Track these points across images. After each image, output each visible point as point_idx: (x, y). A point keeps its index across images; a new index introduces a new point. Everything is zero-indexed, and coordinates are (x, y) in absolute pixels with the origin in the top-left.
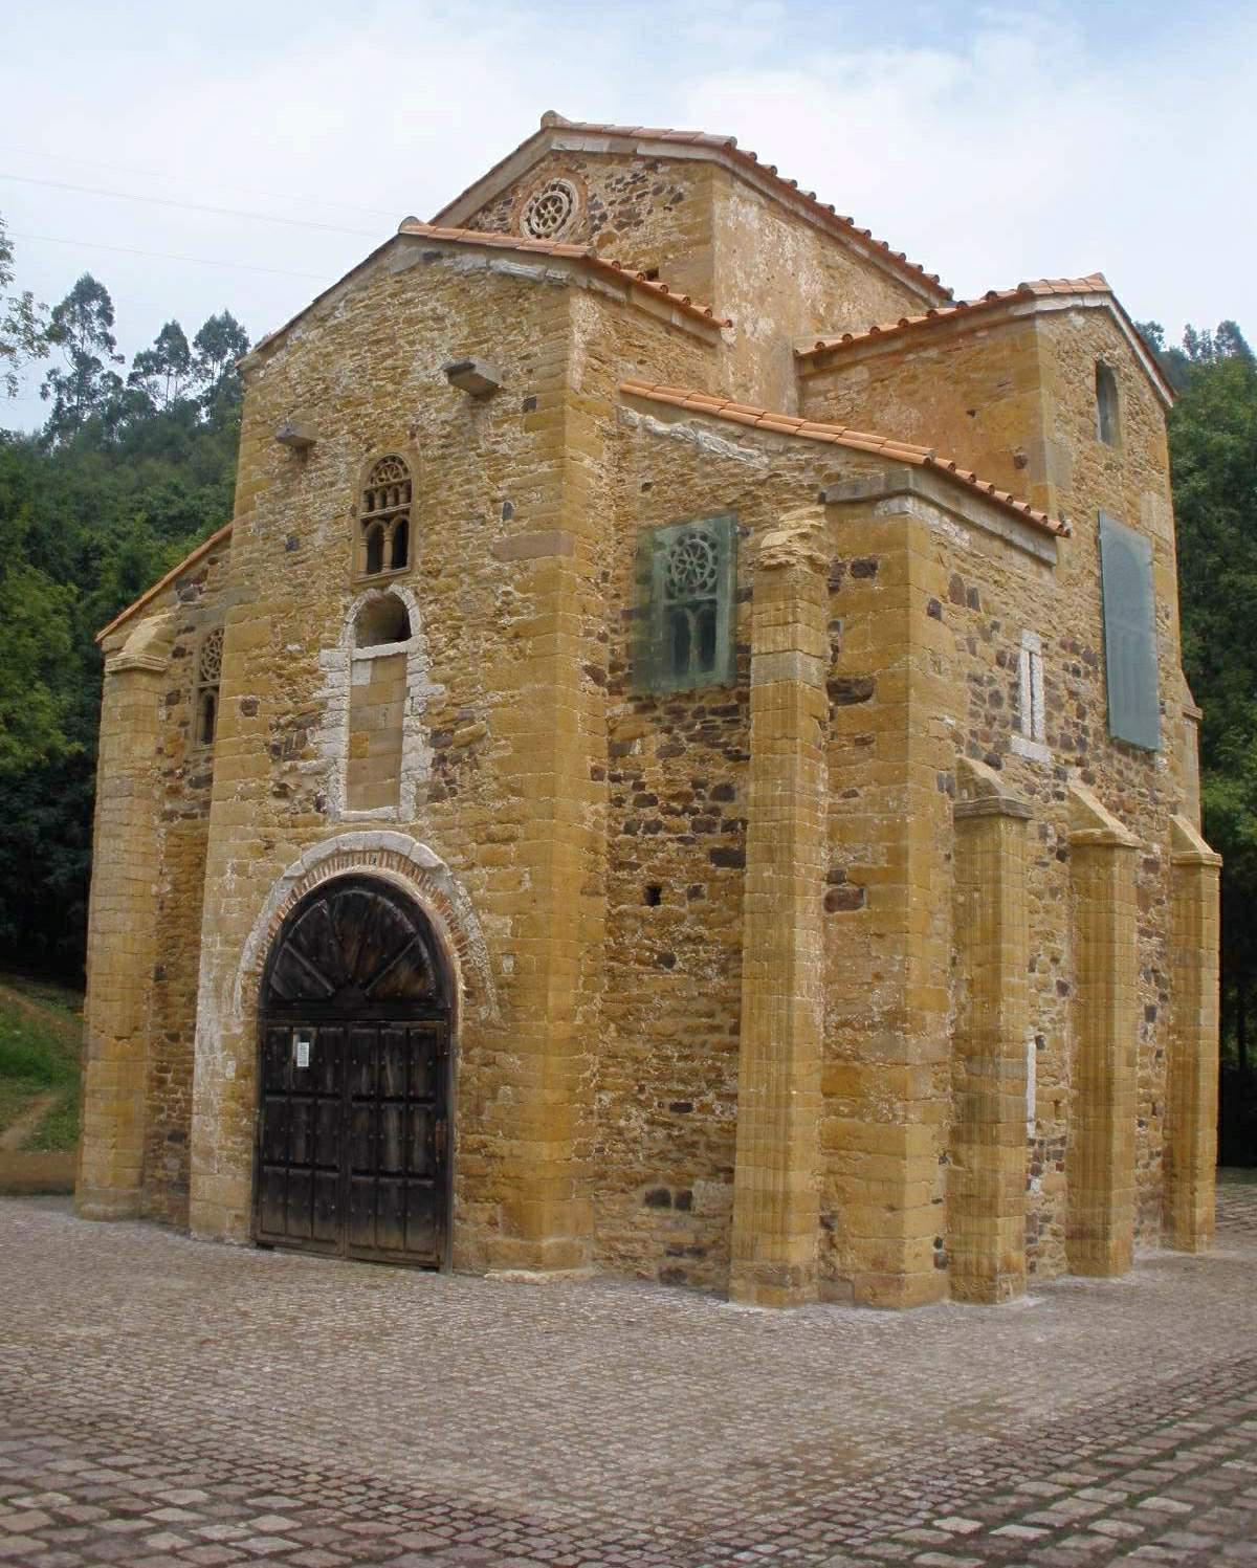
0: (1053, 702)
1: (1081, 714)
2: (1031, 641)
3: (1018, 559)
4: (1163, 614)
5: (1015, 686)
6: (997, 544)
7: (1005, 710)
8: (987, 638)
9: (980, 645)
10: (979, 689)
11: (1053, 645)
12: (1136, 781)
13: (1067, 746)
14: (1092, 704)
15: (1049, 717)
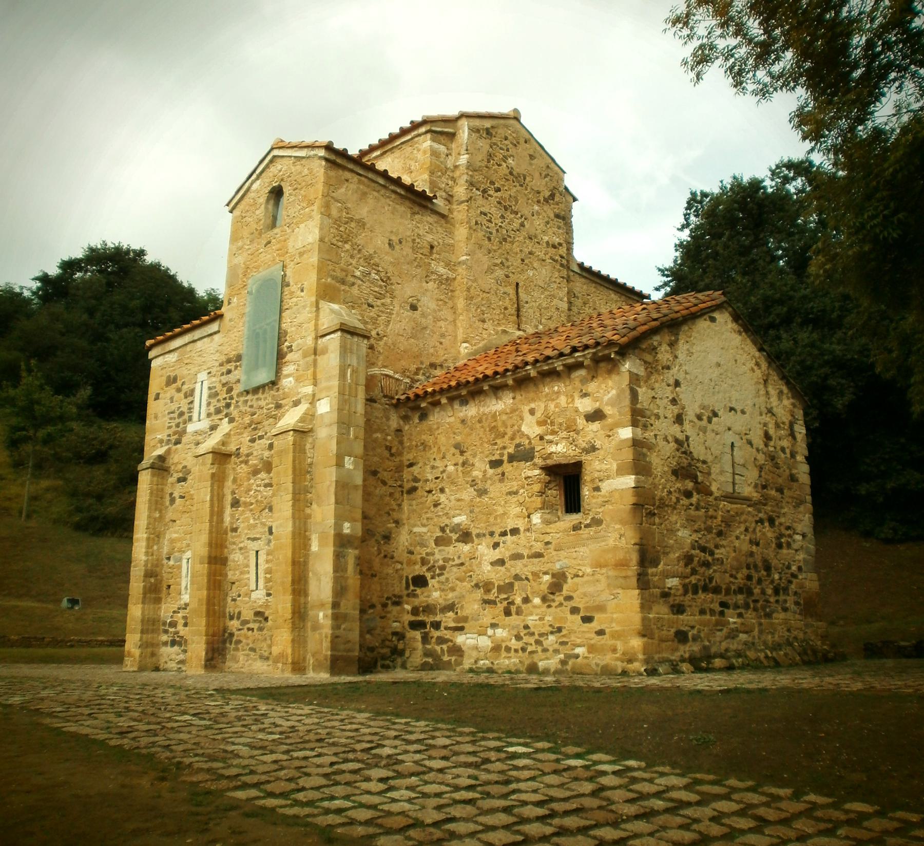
0: (213, 395)
1: (230, 390)
2: (203, 376)
3: (199, 344)
4: (299, 293)
5: (192, 402)
6: (189, 348)
7: (186, 416)
8: (179, 390)
9: (177, 396)
10: (172, 415)
11: (214, 370)
12: (262, 403)
13: (218, 411)
14: (238, 381)
15: (209, 404)
